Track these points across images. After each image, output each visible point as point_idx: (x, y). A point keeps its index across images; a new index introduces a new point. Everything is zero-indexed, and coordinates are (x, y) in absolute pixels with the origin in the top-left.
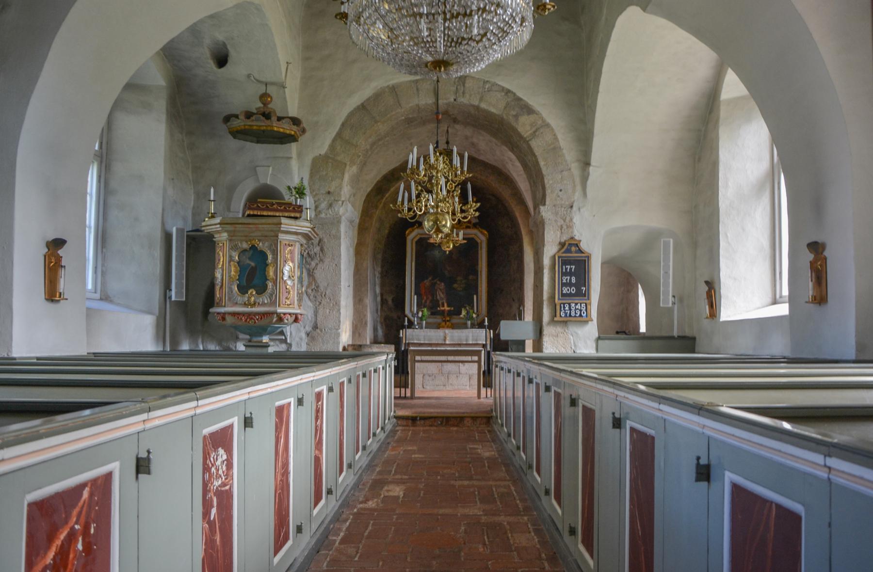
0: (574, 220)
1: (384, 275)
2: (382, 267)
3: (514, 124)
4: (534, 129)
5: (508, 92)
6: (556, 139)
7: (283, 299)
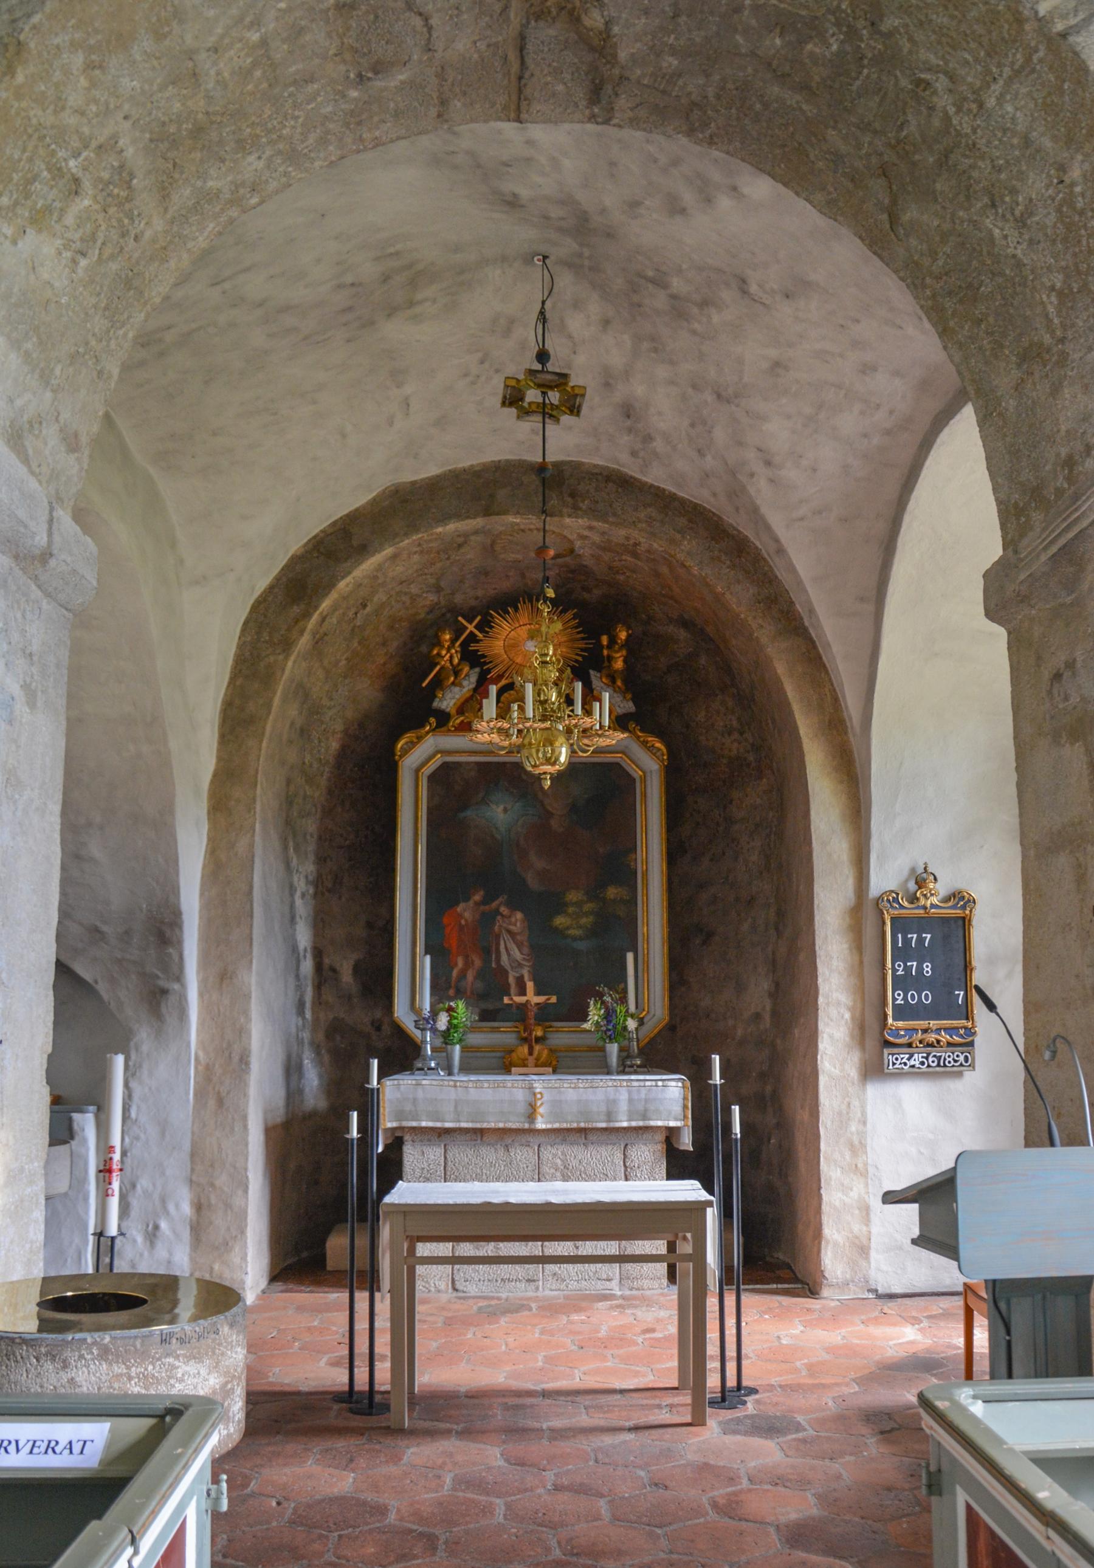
1: (325, 889)
2: (321, 860)
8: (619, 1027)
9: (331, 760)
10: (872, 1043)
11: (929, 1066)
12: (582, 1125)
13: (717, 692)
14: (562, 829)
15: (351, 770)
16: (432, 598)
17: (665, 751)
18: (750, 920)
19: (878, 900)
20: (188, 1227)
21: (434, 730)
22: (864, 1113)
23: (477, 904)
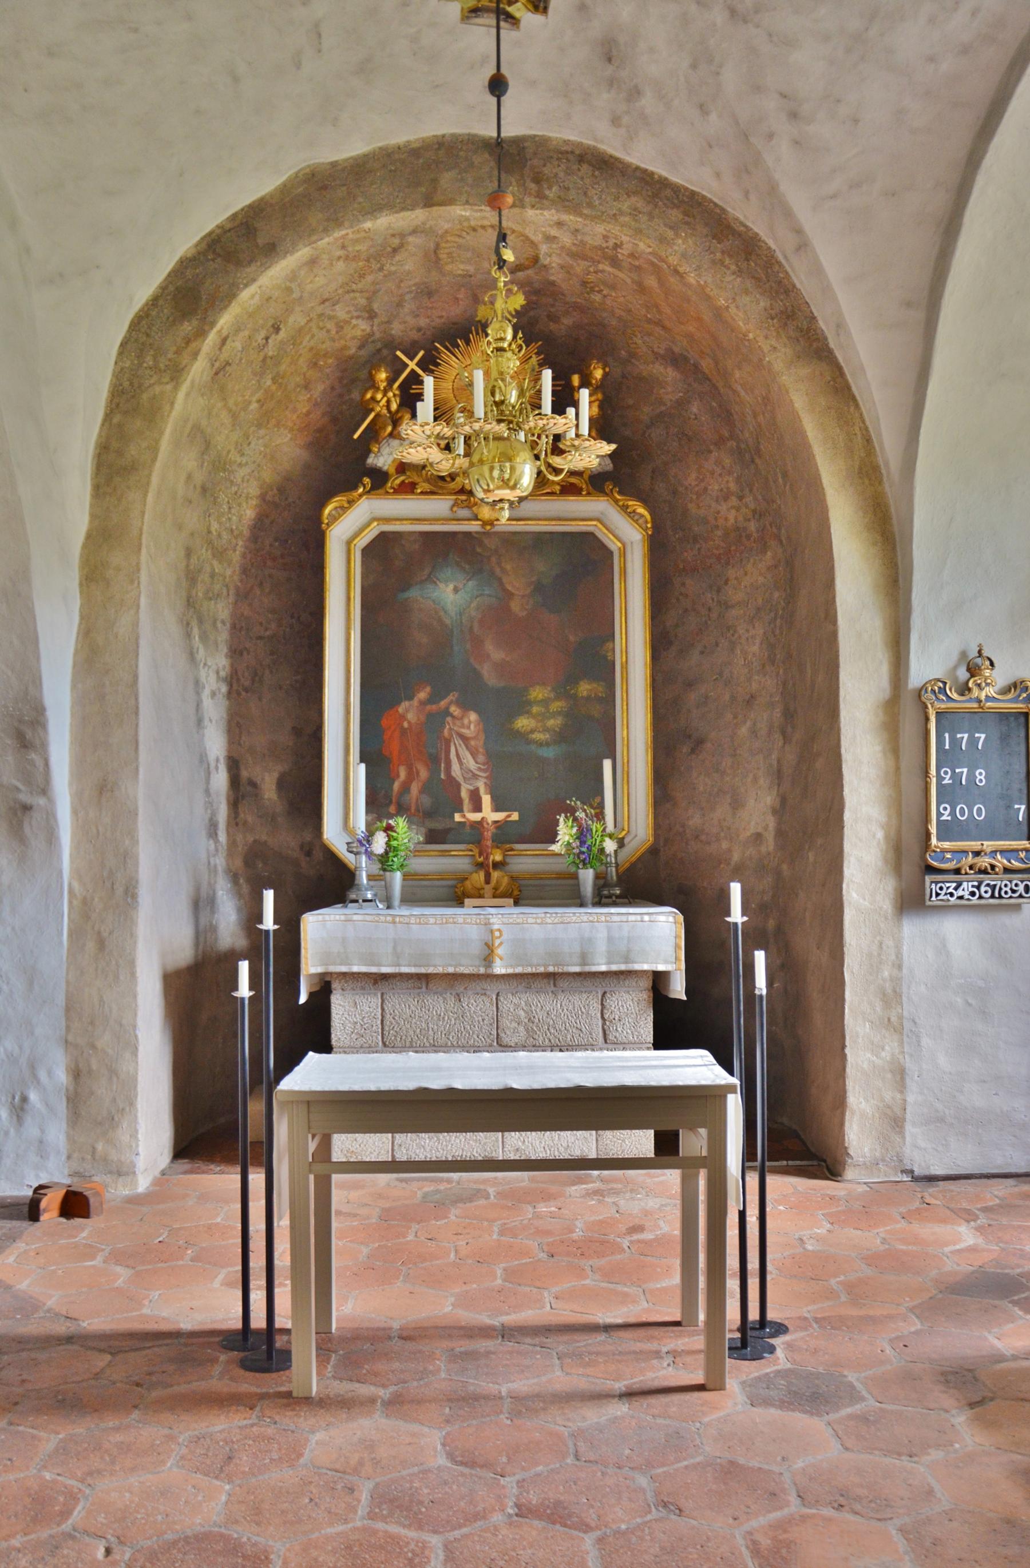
1: (239, 687)
2: (235, 652)
8: (595, 850)
9: (246, 532)
10: (911, 868)
11: (981, 897)
12: (551, 969)
13: (712, 447)
14: (524, 613)
15: (271, 545)
16: (363, 326)
17: (648, 517)
18: (749, 723)
19: (919, 692)
20: (64, 1099)
21: (369, 492)
22: (899, 955)
23: (422, 703)
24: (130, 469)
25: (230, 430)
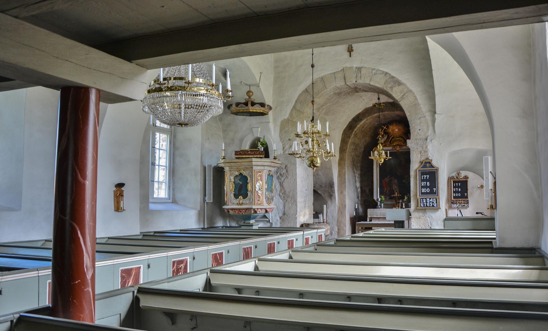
0: (428, 147)
2: (361, 170)
3: (390, 92)
4: (402, 94)
5: (387, 73)
6: (416, 99)
7: (256, 201)
10: (450, 203)
24: (344, 150)
25: (358, 140)
